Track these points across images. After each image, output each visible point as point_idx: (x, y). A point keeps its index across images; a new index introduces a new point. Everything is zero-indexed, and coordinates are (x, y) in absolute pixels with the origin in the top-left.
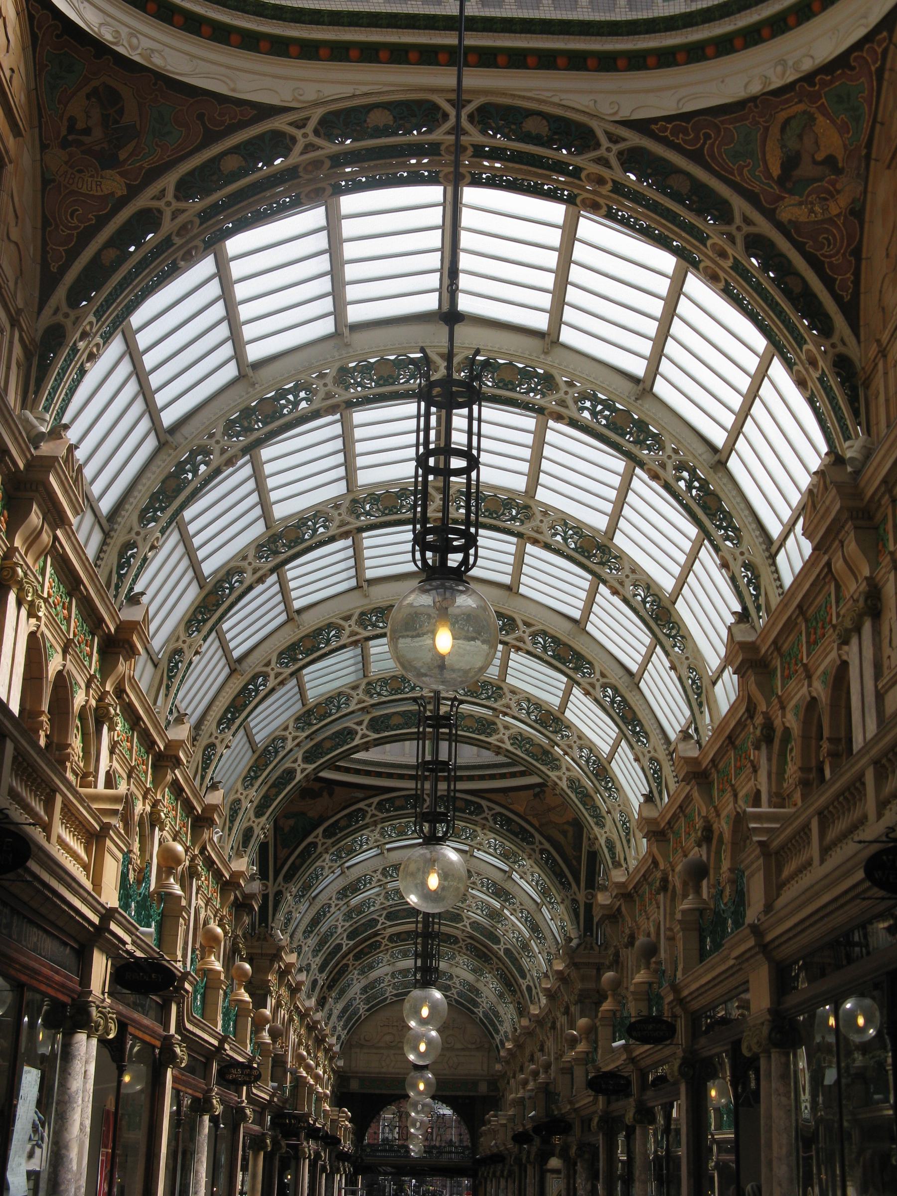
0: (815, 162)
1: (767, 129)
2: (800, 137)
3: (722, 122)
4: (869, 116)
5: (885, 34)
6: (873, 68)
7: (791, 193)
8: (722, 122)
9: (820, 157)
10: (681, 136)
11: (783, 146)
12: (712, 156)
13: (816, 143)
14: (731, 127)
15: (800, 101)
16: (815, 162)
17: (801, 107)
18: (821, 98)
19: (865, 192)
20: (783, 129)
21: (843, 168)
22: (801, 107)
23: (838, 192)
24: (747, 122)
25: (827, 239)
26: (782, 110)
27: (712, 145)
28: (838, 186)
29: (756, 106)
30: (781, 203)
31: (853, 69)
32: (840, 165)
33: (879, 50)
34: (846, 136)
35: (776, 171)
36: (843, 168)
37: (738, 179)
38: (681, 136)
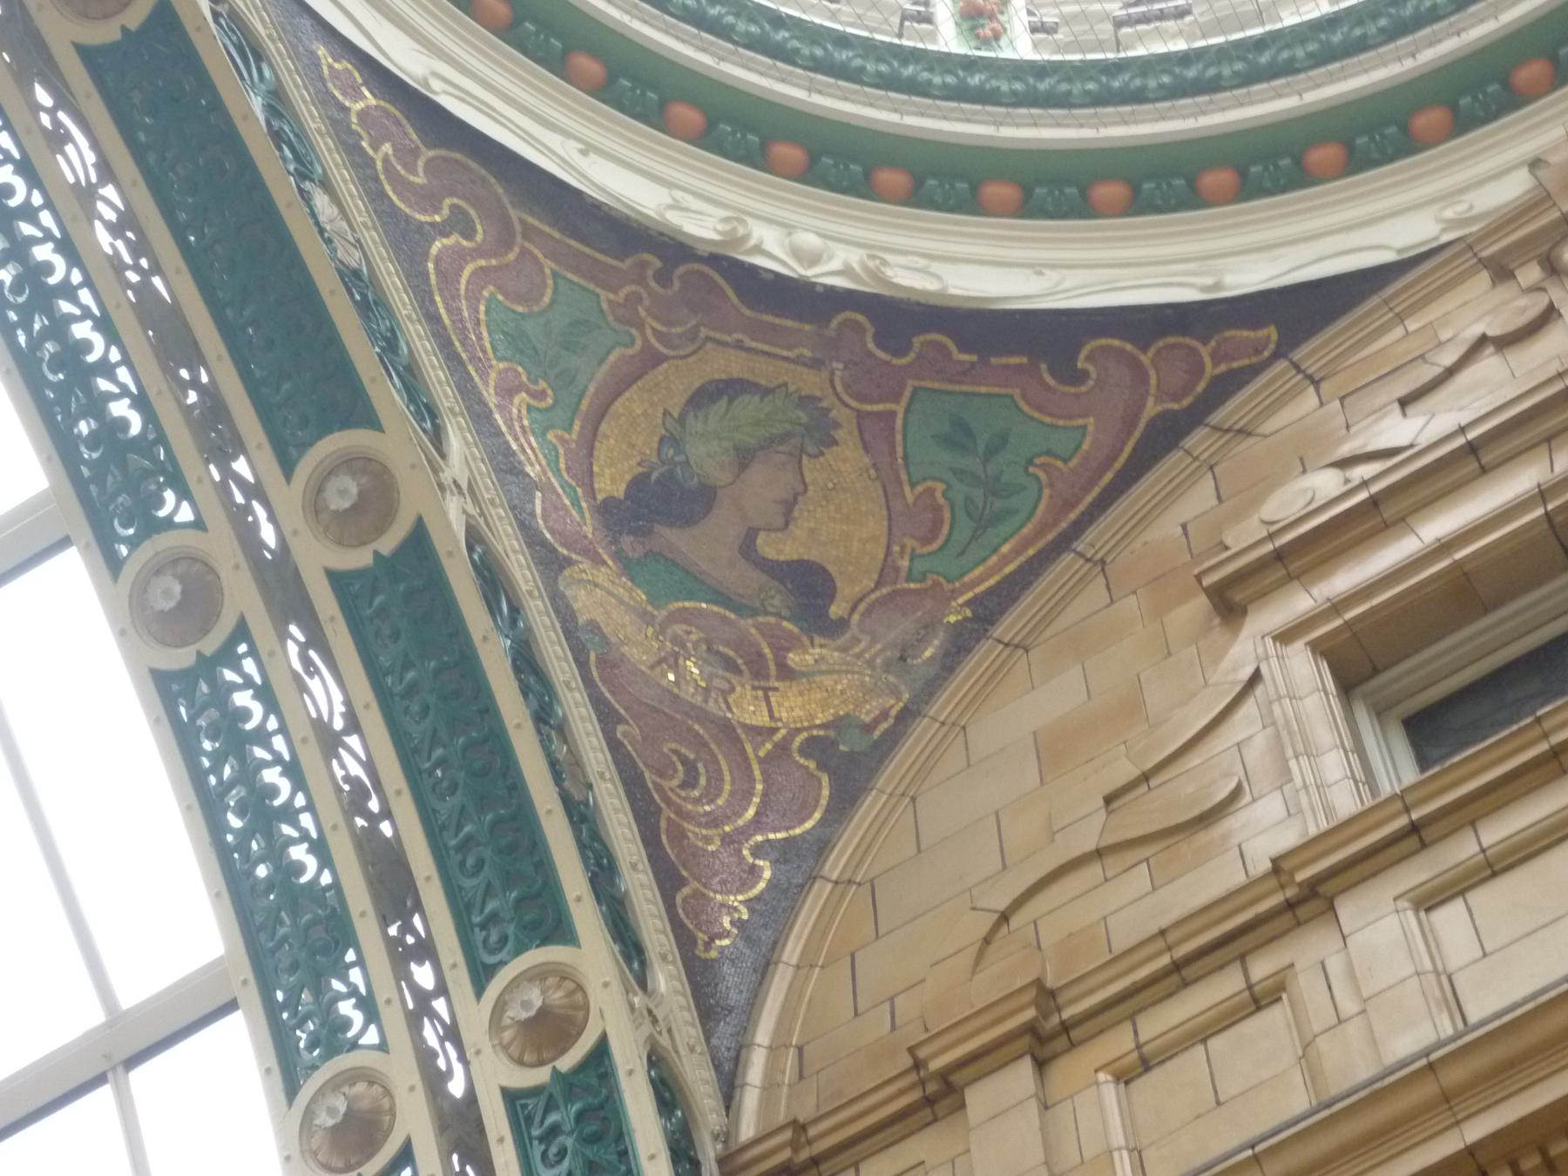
0: (747, 548)
1: (652, 360)
2: (744, 459)
3: (528, 232)
4: (1040, 532)
5: (1272, 332)
6: (1151, 409)
7: (628, 567)
8: (528, 232)
9: (780, 548)
10: (387, 148)
11: (670, 439)
12: (448, 278)
13: (788, 507)
14: (549, 265)
15: (816, 364)
16: (747, 548)
17: (810, 382)
18: (896, 397)
19: (907, 716)
20: (703, 397)
21: (842, 624)
22: (810, 382)
23: (786, 673)
24: (604, 295)
25: (690, 767)
26: (739, 346)
27: (460, 256)
28: (793, 658)
29: (663, 278)
30: (585, 565)
31: (1080, 377)
32: (836, 610)
33: (1210, 371)
34: (910, 543)
35: (611, 483)
36: (842, 624)
37: (491, 399)
38: (387, 148)
